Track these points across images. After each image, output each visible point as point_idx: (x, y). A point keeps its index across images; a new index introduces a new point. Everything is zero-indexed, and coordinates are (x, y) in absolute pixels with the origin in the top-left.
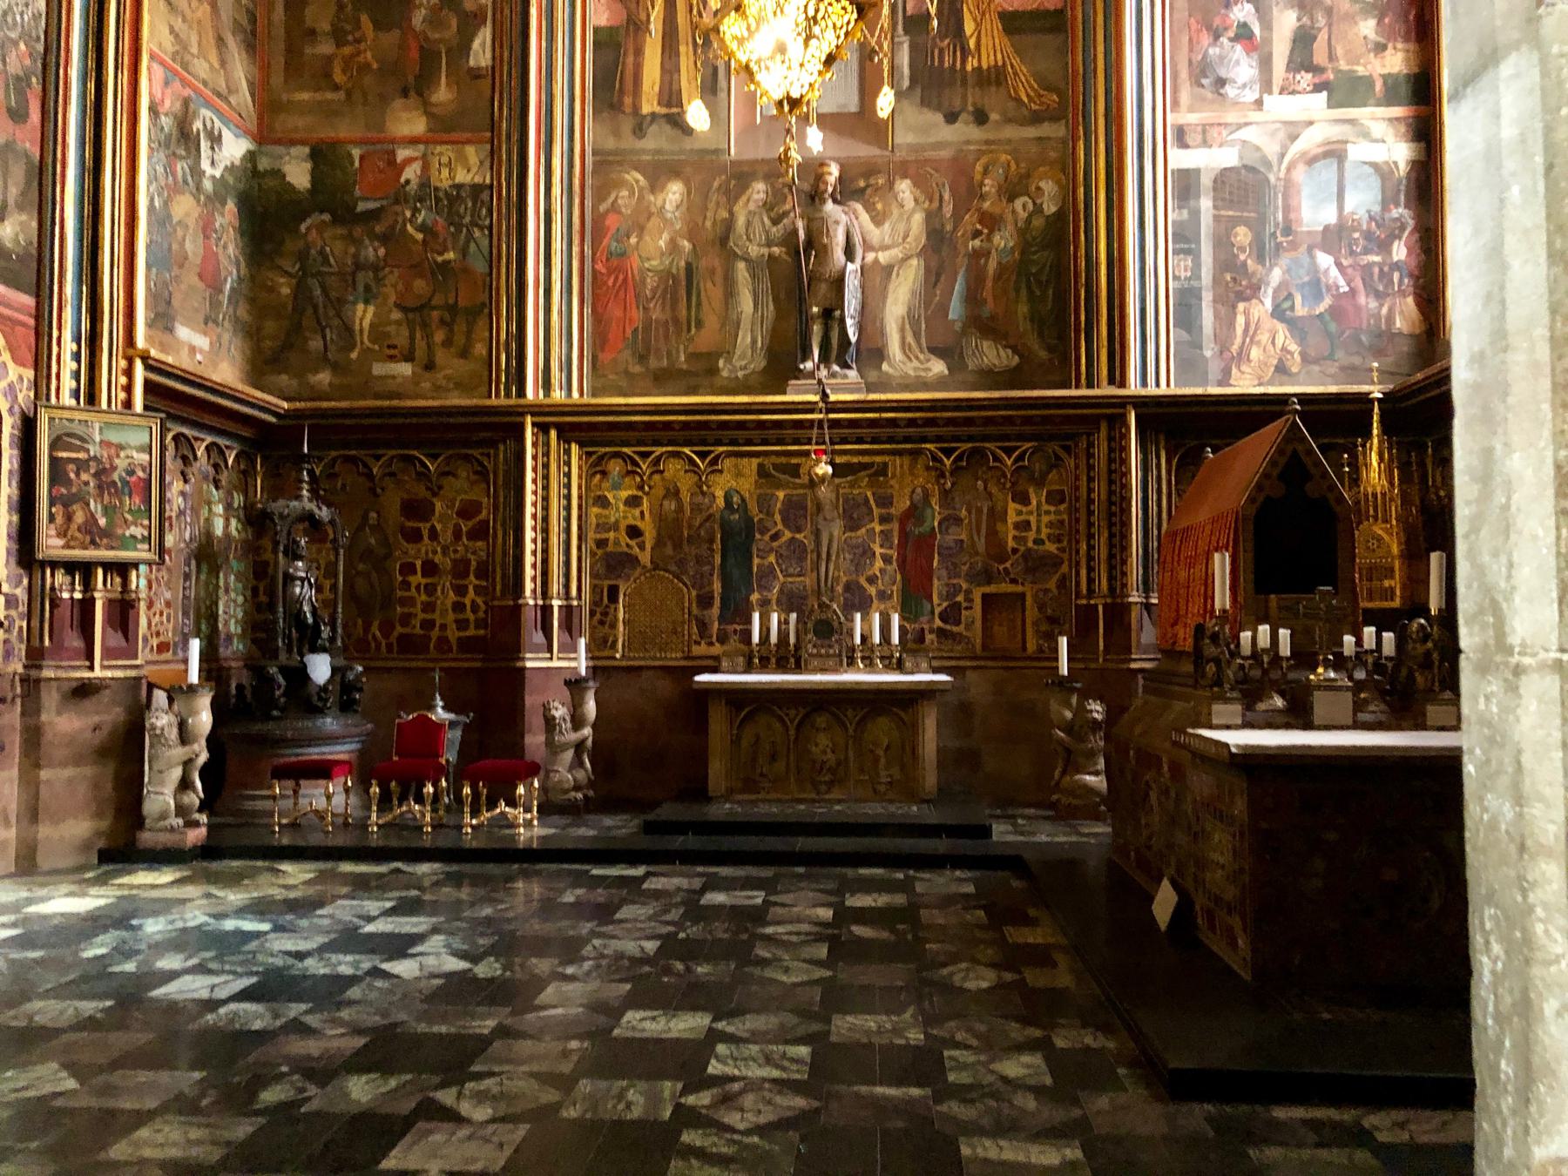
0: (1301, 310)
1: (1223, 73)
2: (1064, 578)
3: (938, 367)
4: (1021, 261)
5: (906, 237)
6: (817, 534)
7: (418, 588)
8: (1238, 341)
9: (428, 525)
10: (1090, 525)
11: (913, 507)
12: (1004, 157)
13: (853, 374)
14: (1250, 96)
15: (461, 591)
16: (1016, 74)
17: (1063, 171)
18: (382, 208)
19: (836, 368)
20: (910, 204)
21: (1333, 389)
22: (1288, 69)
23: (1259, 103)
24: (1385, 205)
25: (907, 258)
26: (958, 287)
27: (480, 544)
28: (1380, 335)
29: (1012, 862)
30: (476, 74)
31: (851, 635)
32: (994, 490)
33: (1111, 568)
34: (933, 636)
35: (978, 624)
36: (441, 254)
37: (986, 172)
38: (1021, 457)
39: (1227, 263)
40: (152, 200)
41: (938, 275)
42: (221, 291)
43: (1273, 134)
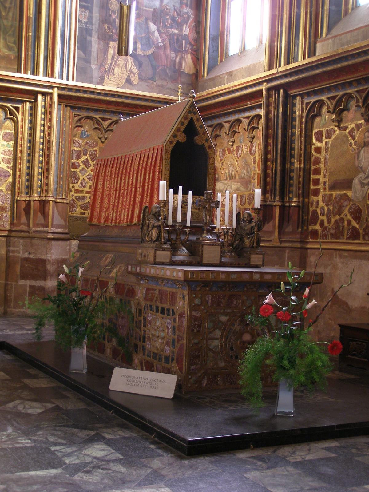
8: (109, 62)
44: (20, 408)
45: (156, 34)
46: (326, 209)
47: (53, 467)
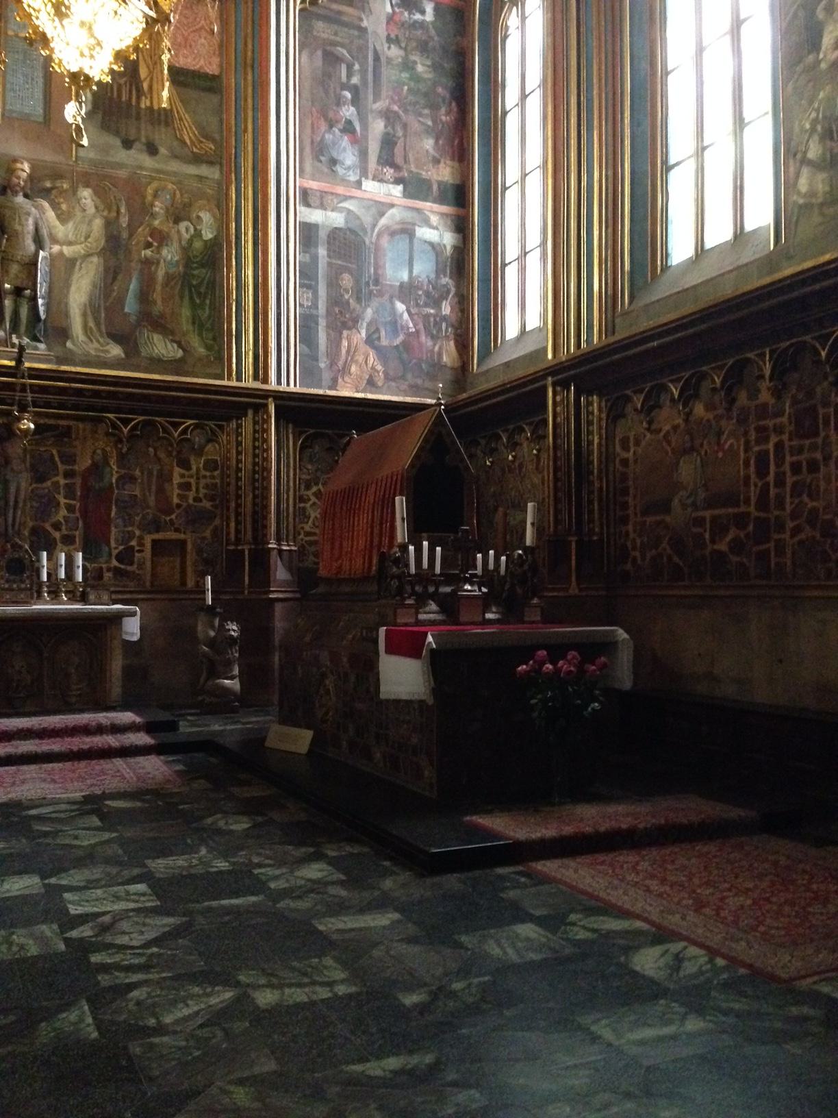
0: (384, 342)
1: (335, 155)
2: (216, 528)
3: (116, 351)
4: (185, 273)
5: (87, 237)
10: (238, 488)
11: (95, 465)
12: (170, 186)
14: (353, 178)
16: (181, 119)
17: (218, 207)
19: (26, 340)
20: (91, 210)
21: (409, 399)
22: (379, 163)
23: (359, 184)
24: (439, 272)
25: (89, 255)
26: (133, 286)
28: (434, 365)
29: (207, 745)
31: (38, 572)
32: (162, 455)
33: (255, 521)
34: (110, 574)
35: (148, 564)
37: (155, 196)
38: (185, 431)
39: (336, 301)
41: (116, 274)
43: (368, 208)
44: (221, 824)
45: (406, 316)
46: (638, 541)
47: (253, 894)
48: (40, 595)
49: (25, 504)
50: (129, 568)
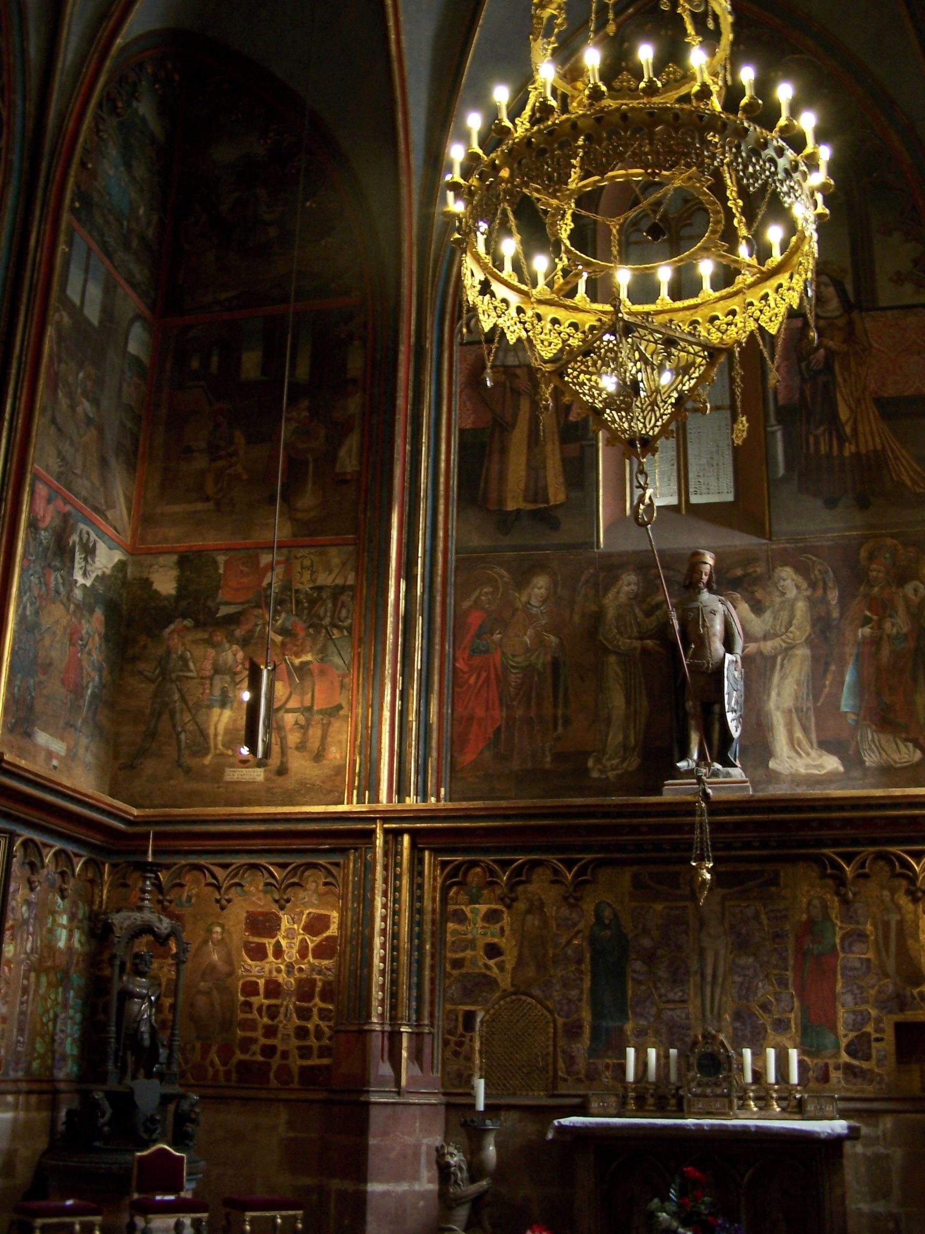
3: (832, 763)
6: (702, 953)
7: (260, 1010)
9: (274, 941)
12: (889, 541)
13: (737, 773)
15: (304, 1014)
16: (896, 458)
18: (240, 613)
19: (718, 766)
27: (325, 962)
30: (341, 481)
31: (741, 1069)
36: (297, 655)
37: (871, 557)
40: (25, 608)
41: (827, 664)
42: (82, 697)
48: (744, 1107)
49: (725, 978)
50: (865, 1065)
